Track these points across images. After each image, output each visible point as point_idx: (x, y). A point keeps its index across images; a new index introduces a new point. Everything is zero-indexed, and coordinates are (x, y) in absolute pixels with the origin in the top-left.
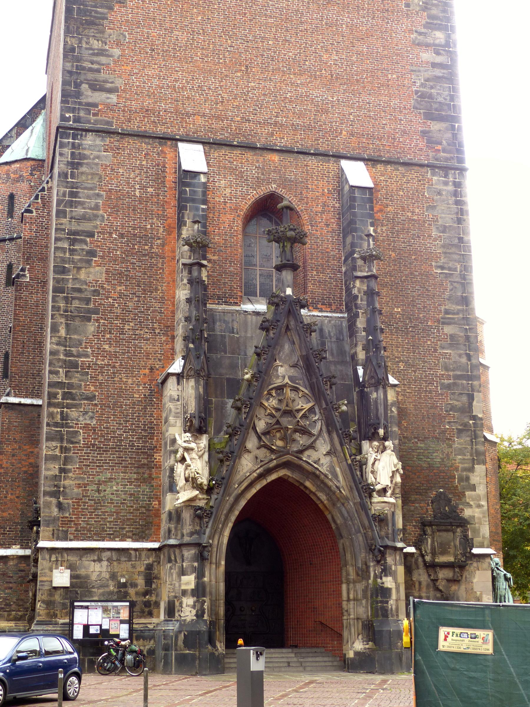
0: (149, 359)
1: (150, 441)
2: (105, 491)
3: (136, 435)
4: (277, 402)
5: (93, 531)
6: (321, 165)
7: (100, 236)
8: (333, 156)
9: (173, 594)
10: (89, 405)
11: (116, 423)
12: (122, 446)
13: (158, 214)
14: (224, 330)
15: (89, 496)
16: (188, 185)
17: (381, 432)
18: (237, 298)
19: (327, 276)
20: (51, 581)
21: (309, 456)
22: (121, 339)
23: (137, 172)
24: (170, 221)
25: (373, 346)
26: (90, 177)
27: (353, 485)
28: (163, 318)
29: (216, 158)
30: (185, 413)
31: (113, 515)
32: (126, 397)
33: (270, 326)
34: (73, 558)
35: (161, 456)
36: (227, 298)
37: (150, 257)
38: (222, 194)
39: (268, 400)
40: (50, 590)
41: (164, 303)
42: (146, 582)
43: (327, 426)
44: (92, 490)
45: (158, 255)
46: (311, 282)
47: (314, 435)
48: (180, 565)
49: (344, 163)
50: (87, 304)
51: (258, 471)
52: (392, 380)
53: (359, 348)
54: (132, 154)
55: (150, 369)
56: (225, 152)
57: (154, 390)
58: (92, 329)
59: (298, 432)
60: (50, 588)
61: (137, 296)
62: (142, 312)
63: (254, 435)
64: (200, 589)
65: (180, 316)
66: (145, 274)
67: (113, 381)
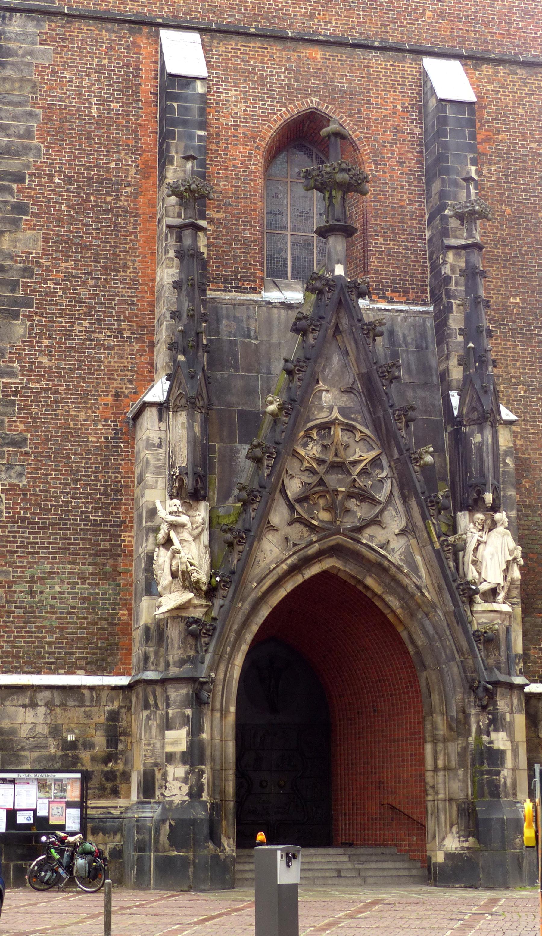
0: (114, 379)
1: (114, 512)
2: (42, 592)
3: (92, 503)
4: (320, 449)
5: (22, 658)
6: (391, 65)
7: (34, 181)
8: (410, 51)
9: (152, 760)
10: (17, 455)
11: (60, 484)
12: (69, 519)
13: (128, 146)
14: (235, 333)
15: (15, 602)
16: (176, 98)
17: (489, 497)
18: (256, 281)
19: (401, 245)
21: (372, 537)
22: (68, 348)
23: (94, 76)
24: (147, 156)
25: (476, 359)
26: (17, 85)
27: (443, 583)
28: (136, 314)
29: (221, 55)
30: (171, 466)
31: (55, 633)
32: (75, 441)
33: (309, 326)
35: (132, 537)
36: (240, 280)
37: (114, 215)
38: (231, 113)
39: (305, 445)
41: (137, 288)
43: (401, 487)
44: (21, 592)
45: (128, 212)
46: (375, 255)
47: (380, 503)
48: (164, 713)
49: (428, 63)
50: (13, 291)
51: (289, 561)
52: (506, 414)
53: (453, 362)
54: (86, 49)
55: (115, 396)
56: (236, 45)
57: (121, 430)
58: (21, 331)
59: (354, 497)
61: (93, 278)
62: (102, 303)
63: (283, 502)
64: (196, 751)
65: (163, 309)
66: (107, 242)
67: (55, 415)
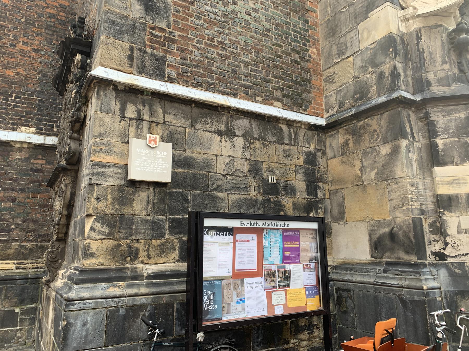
20: (125, 167)
34: (176, 120)
40: (120, 189)
42: (307, 186)
60: (122, 182)
